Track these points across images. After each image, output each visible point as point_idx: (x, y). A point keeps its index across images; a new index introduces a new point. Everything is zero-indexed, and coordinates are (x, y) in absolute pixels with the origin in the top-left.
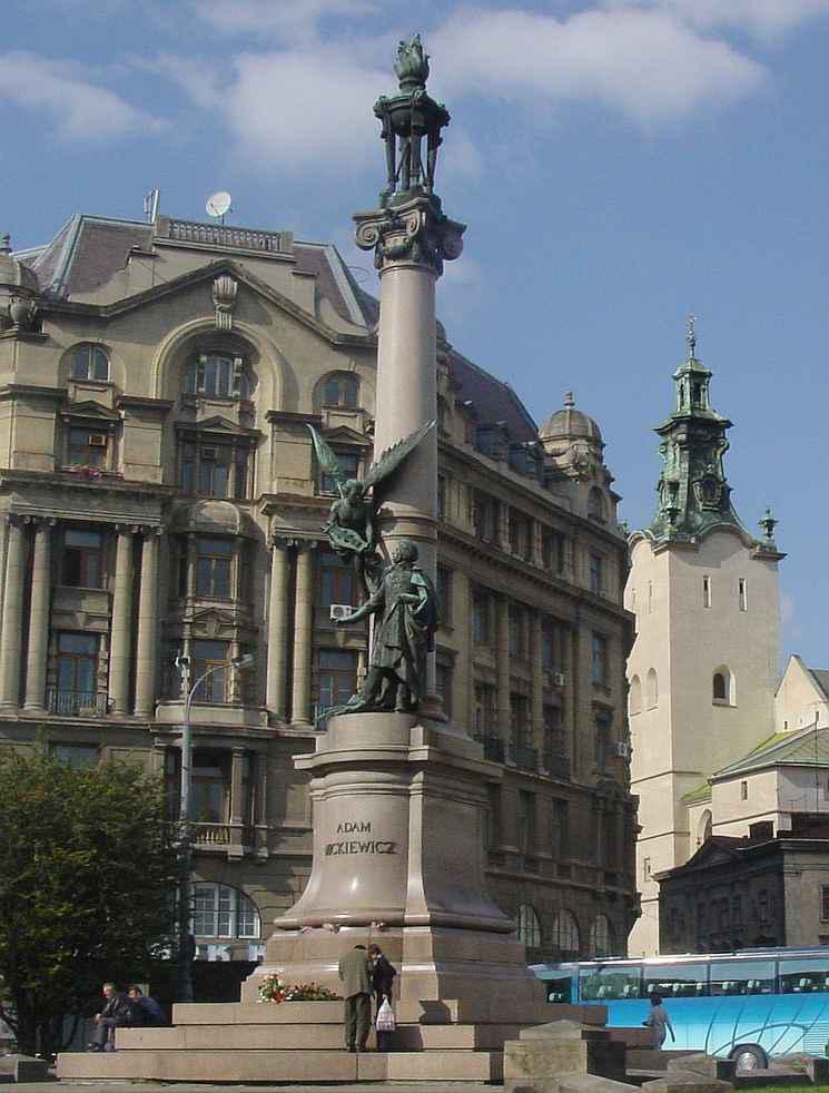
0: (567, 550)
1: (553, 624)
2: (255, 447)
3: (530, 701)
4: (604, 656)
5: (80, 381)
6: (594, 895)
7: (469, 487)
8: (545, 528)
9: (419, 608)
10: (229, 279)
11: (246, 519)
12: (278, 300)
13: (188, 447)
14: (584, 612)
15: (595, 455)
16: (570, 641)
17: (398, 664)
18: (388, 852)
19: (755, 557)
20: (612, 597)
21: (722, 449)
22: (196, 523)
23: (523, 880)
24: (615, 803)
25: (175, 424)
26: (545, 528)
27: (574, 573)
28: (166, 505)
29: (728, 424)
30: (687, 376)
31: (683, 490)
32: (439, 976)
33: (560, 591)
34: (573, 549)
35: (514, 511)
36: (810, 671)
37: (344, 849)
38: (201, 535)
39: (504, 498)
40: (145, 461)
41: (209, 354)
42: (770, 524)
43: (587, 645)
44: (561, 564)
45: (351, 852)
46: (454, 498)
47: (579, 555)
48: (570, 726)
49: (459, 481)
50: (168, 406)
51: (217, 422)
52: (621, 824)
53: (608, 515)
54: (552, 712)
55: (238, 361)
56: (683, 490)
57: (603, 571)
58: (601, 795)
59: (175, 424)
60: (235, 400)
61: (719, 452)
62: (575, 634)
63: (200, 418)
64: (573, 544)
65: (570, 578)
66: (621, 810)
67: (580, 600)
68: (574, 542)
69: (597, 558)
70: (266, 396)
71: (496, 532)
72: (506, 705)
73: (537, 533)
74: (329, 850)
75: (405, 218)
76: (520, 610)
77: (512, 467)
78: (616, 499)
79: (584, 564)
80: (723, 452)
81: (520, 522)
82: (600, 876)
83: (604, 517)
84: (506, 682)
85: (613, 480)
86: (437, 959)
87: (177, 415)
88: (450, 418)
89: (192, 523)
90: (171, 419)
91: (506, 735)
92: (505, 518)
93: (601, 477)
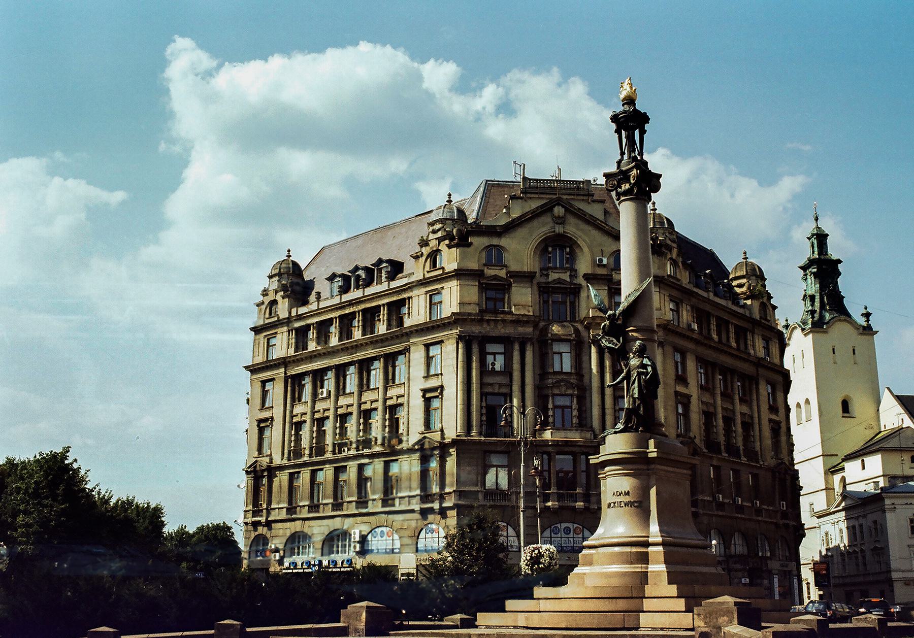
0: (749, 337)
1: (743, 377)
2: (579, 292)
5: (488, 264)
6: (776, 525)
8: (736, 326)
10: (560, 207)
11: (577, 331)
12: (585, 216)
13: (546, 295)
14: (761, 371)
19: (861, 334)
20: (777, 361)
22: (552, 334)
23: (736, 518)
25: (538, 283)
26: (737, 327)
27: (754, 350)
28: (536, 326)
29: (839, 261)
30: (815, 237)
31: (817, 300)
32: (667, 572)
35: (719, 319)
36: (896, 396)
37: (616, 504)
38: (553, 340)
40: (524, 303)
41: (552, 247)
42: (867, 315)
43: (765, 390)
45: (620, 507)
46: (685, 313)
47: (757, 341)
48: (757, 433)
50: (534, 275)
51: (560, 281)
53: (770, 317)
55: (568, 250)
56: (817, 300)
59: (538, 283)
60: (567, 269)
61: (836, 277)
63: (550, 279)
66: (788, 477)
67: (759, 363)
68: (753, 333)
69: (767, 340)
70: (584, 266)
71: (709, 330)
72: (720, 422)
73: (732, 329)
74: (609, 506)
76: (727, 372)
77: (716, 295)
78: (774, 308)
79: (759, 344)
80: (838, 277)
81: (722, 325)
82: (779, 515)
83: (768, 318)
84: (719, 410)
85: (772, 297)
86: (666, 562)
87: (538, 278)
88: (680, 272)
89: (550, 335)
90: (535, 282)
91: (722, 439)
92: (713, 322)
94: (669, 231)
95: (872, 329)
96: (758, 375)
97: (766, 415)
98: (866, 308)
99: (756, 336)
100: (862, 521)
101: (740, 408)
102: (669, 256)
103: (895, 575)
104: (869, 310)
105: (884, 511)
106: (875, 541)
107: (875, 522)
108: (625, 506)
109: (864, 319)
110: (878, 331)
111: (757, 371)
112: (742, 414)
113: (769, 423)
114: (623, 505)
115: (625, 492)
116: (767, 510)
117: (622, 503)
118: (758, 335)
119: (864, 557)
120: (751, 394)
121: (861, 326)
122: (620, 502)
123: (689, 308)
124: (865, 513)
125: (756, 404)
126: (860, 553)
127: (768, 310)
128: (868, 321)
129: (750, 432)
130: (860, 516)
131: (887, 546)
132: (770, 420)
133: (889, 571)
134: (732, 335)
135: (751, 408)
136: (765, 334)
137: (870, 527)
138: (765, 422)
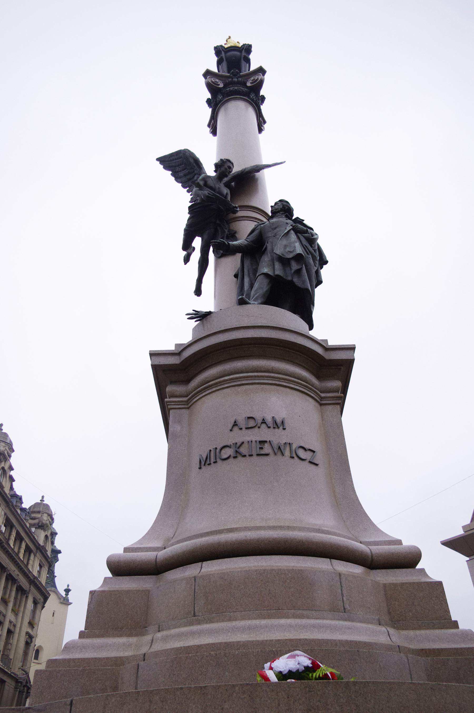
3: (3, 624)
4: (34, 612)
7: (5, 514)
15: (50, 522)
16: (24, 600)
17: (298, 272)
18: (310, 462)
19: (61, 603)
21: (56, 561)
24: (24, 686)
26: (27, 546)
29: (60, 552)
33: (26, 574)
34: (34, 558)
37: (243, 450)
39: (16, 526)
42: (67, 591)
44: (28, 563)
45: (258, 455)
47: (36, 562)
49: (2, 509)
52: (24, 696)
53: (48, 549)
54: (10, 632)
57: (42, 572)
58: (20, 681)
62: (27, 597)
64: (35, 556)
65: (31, 571)
67: (33, 582)
76: (10, 579)
80: (56, 562)
81: (19, 538)
83: (47, 548)
92: (14, 534)
94: (9, 446)
95: (68, 600)
96: (30, 590)
97: (26, 628)
98: (68, 586)
99: (36, 559)
101: (10, 616)
104: (70, 588)
108: (275, 454)
109: (65, 593)
110: (71, 603)
111: (30, 587)
112: (10, 622)
113: (26, 635)
117: (266, 446)
118: (38, 558)
120: (19, 606)
121: (62, 596)
127: (48, 543)
128: (67, 595)
129: (10, 639)
132: (27, 633)
134: (22, 551)
135: (16, 619)
136: (42, 561)
138: (23, 634)
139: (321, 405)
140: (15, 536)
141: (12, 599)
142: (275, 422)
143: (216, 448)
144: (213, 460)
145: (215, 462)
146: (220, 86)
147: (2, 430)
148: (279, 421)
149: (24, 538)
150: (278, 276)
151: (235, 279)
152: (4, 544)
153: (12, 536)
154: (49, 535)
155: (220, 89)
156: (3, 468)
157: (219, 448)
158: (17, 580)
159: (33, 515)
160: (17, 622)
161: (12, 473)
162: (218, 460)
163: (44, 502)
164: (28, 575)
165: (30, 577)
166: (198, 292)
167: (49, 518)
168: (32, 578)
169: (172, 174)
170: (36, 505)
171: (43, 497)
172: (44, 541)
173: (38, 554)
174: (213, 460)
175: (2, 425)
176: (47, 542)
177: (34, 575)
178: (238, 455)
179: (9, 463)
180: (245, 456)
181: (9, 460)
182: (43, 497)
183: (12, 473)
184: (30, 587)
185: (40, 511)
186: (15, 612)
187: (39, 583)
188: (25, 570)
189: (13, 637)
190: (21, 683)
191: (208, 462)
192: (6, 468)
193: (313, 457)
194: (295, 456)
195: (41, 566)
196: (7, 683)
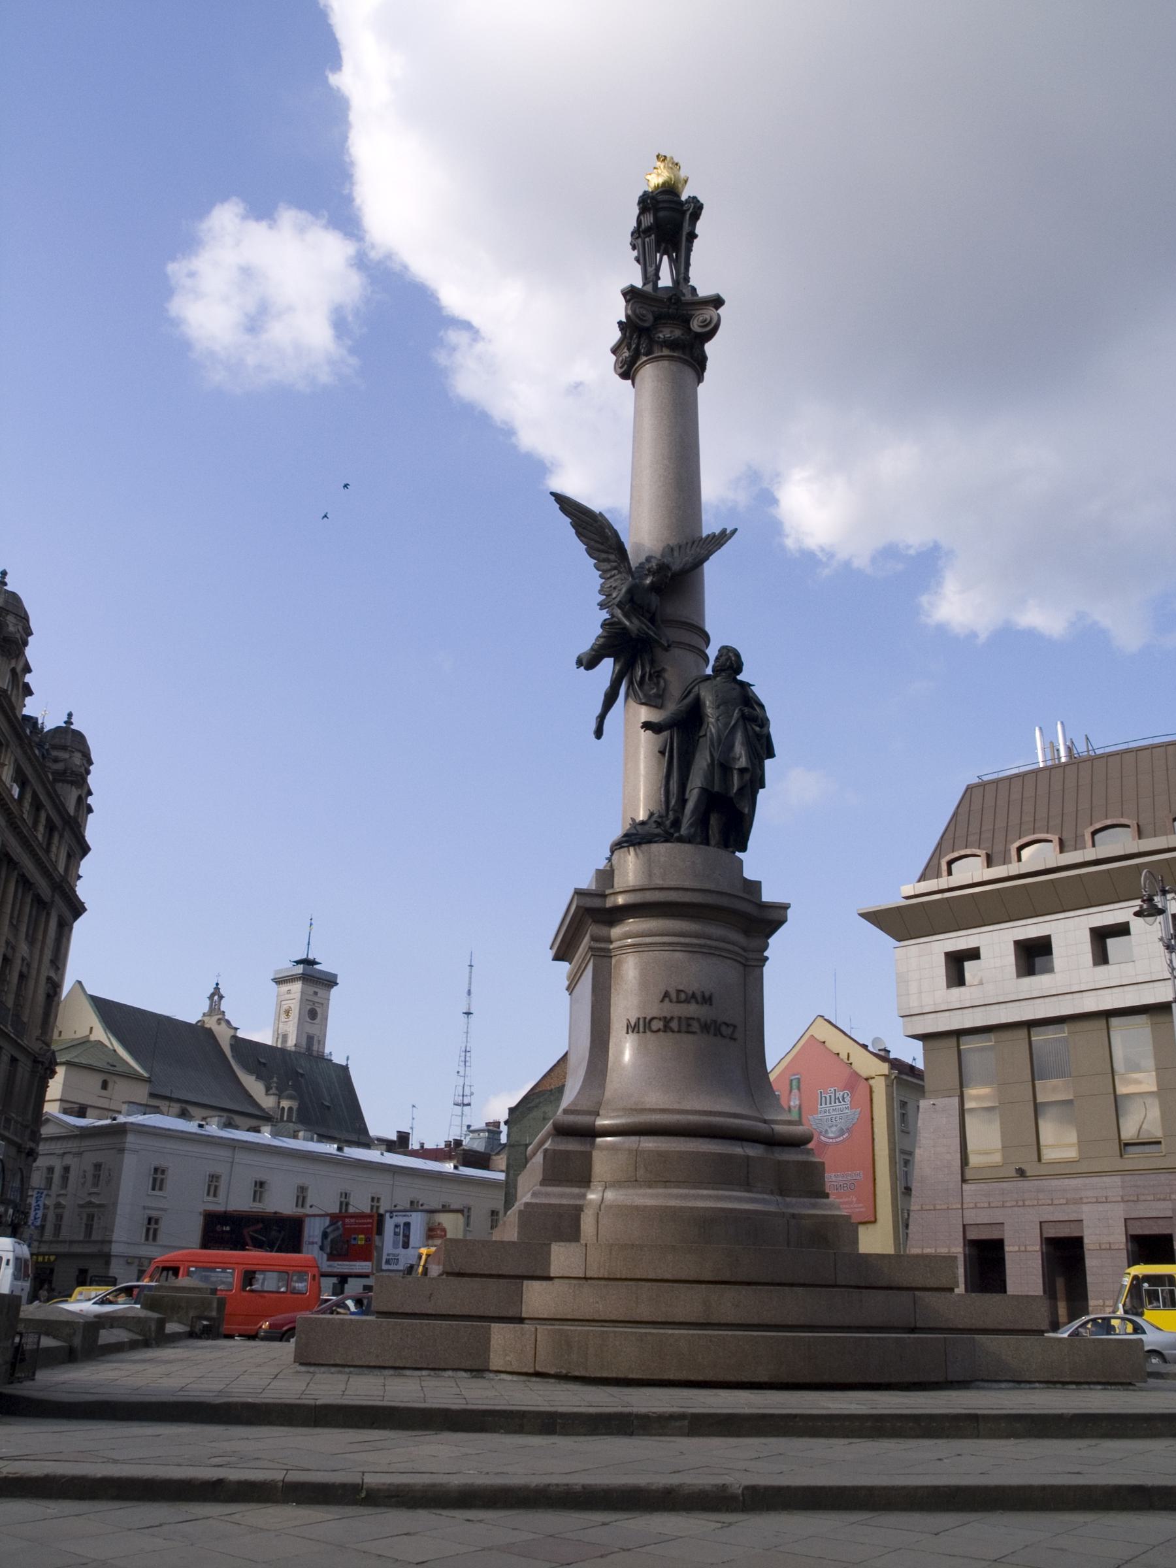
7: (16, 760)
9: (765, 730)
14: (57, 898)
24: (47, 1069)
26: (49, 819)
33: (47, 874)
34: (59, 842)
35: (35, 796)
37: (674, 1025)
45: (688, 1032)
54: (22, 977)
62: (48, 914)
68: (61, 836)
75: (689, 312)
76: (25, 883)
78: (90, 810)
81: (37, 806)
88: (18, 695)
93: (85, 791)
96: (53, 901)
100: (68, 1160)
101: (23, 949)
102: (13, 665)
103: (116, 1249)
105: (122, 1151)
106: (90, 1194)
107: (98, 1166)
108: (702, 1032)
111: (53, 896)
112: (23, 959)
113: (47, 983)
114: (695, 1026)
115: (703, 997)
116: (17, 1122)
118: (66, 842)
119: (59, 1217)
122: (688, 1019)
123: (13, 759)
124: (82, 1149)
125: (39, 947)
126: (52, 1208)
130: (70, 1152)
131: (115, 1204)
133: (110, 1242)
134: (41, 828)
137: (85, 1171)
139: (745, 966)
140: (30, 800)
141: (25, 919)
142: (703, 997)
143: (645, 1018)
144: (641, 1029)
145: (645, 1032)
146: (646, 325)
147: (6, 584)
148: (707, 994)
149: (45, 803)
150: (717, 792)
151: (658, 754)
152: (16, 820)
153: (26, 801)
154: (83, 796)
155: (648, 330)
156: (13, 671)
157: (648, 1018)
158: (34, 884)
159: (55, 753)
160: (31, 957)
161: (28, 678)
162: (647, 1030)
163: (72, 727)
164: (51, 875)
165: (53, 879)
166: (599, 733)
167: (85, 762)
168: (58, 880)
169: (571, 523)
170: (58, 729)
171: (70, 715)
172: (75, 807)
173: (65, 833)
174: (641, 1029)
175: (4, 573)
176: (79, 808)
177: (61, 875)
178: (668, 1030)
179: (23, 658)
180: (673, 1031)
181: (24, 653)
182: (70, 715)
183: (28, 678)
184: (53, 896)
185: (68, 746)
186: (31, 941)
187: (70, 890)
188: (48, 865)
189: (26, 985)
190: (42, 1063)
191: (636, 1030)
192: (19, 669)
193: (733, 1032)
194: (718, 1032)
195: (69, 856)
196: (20, 1064)
